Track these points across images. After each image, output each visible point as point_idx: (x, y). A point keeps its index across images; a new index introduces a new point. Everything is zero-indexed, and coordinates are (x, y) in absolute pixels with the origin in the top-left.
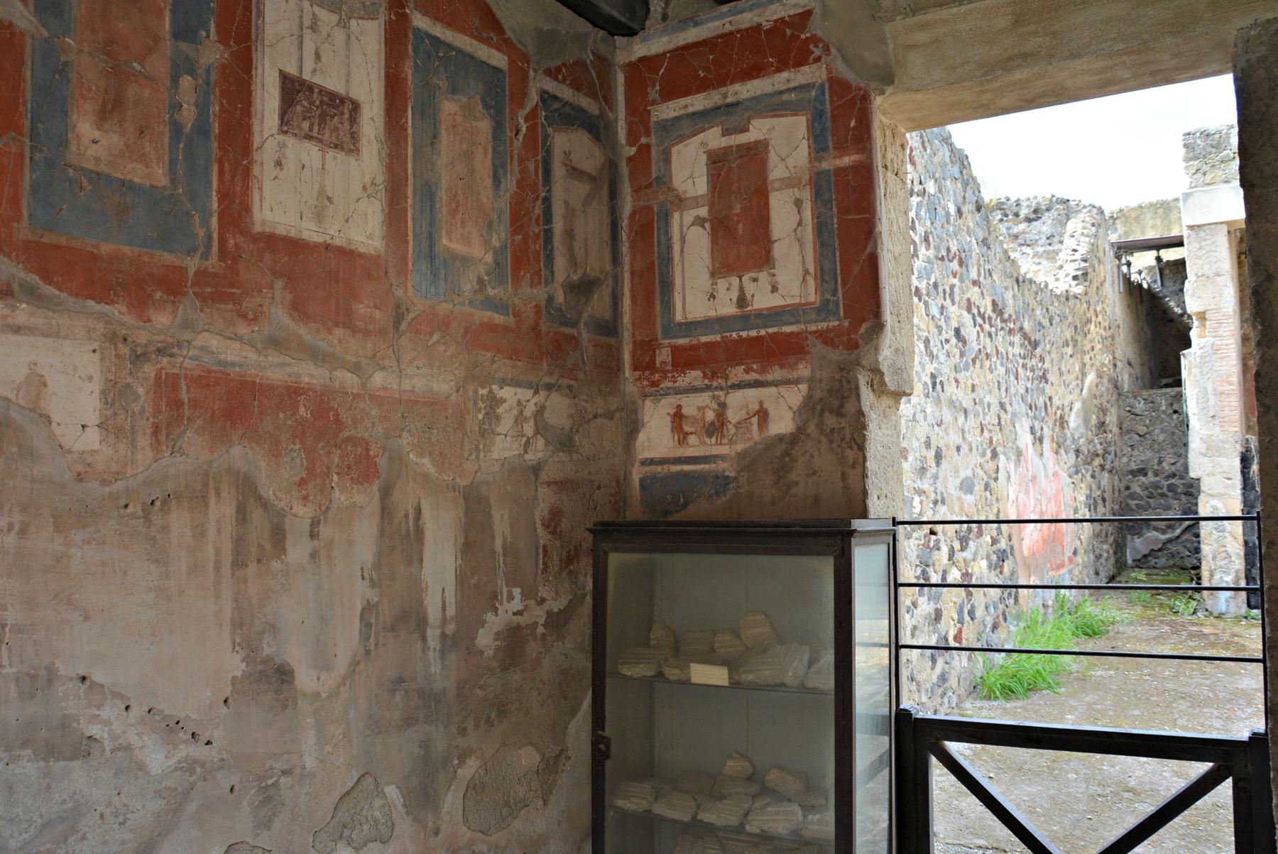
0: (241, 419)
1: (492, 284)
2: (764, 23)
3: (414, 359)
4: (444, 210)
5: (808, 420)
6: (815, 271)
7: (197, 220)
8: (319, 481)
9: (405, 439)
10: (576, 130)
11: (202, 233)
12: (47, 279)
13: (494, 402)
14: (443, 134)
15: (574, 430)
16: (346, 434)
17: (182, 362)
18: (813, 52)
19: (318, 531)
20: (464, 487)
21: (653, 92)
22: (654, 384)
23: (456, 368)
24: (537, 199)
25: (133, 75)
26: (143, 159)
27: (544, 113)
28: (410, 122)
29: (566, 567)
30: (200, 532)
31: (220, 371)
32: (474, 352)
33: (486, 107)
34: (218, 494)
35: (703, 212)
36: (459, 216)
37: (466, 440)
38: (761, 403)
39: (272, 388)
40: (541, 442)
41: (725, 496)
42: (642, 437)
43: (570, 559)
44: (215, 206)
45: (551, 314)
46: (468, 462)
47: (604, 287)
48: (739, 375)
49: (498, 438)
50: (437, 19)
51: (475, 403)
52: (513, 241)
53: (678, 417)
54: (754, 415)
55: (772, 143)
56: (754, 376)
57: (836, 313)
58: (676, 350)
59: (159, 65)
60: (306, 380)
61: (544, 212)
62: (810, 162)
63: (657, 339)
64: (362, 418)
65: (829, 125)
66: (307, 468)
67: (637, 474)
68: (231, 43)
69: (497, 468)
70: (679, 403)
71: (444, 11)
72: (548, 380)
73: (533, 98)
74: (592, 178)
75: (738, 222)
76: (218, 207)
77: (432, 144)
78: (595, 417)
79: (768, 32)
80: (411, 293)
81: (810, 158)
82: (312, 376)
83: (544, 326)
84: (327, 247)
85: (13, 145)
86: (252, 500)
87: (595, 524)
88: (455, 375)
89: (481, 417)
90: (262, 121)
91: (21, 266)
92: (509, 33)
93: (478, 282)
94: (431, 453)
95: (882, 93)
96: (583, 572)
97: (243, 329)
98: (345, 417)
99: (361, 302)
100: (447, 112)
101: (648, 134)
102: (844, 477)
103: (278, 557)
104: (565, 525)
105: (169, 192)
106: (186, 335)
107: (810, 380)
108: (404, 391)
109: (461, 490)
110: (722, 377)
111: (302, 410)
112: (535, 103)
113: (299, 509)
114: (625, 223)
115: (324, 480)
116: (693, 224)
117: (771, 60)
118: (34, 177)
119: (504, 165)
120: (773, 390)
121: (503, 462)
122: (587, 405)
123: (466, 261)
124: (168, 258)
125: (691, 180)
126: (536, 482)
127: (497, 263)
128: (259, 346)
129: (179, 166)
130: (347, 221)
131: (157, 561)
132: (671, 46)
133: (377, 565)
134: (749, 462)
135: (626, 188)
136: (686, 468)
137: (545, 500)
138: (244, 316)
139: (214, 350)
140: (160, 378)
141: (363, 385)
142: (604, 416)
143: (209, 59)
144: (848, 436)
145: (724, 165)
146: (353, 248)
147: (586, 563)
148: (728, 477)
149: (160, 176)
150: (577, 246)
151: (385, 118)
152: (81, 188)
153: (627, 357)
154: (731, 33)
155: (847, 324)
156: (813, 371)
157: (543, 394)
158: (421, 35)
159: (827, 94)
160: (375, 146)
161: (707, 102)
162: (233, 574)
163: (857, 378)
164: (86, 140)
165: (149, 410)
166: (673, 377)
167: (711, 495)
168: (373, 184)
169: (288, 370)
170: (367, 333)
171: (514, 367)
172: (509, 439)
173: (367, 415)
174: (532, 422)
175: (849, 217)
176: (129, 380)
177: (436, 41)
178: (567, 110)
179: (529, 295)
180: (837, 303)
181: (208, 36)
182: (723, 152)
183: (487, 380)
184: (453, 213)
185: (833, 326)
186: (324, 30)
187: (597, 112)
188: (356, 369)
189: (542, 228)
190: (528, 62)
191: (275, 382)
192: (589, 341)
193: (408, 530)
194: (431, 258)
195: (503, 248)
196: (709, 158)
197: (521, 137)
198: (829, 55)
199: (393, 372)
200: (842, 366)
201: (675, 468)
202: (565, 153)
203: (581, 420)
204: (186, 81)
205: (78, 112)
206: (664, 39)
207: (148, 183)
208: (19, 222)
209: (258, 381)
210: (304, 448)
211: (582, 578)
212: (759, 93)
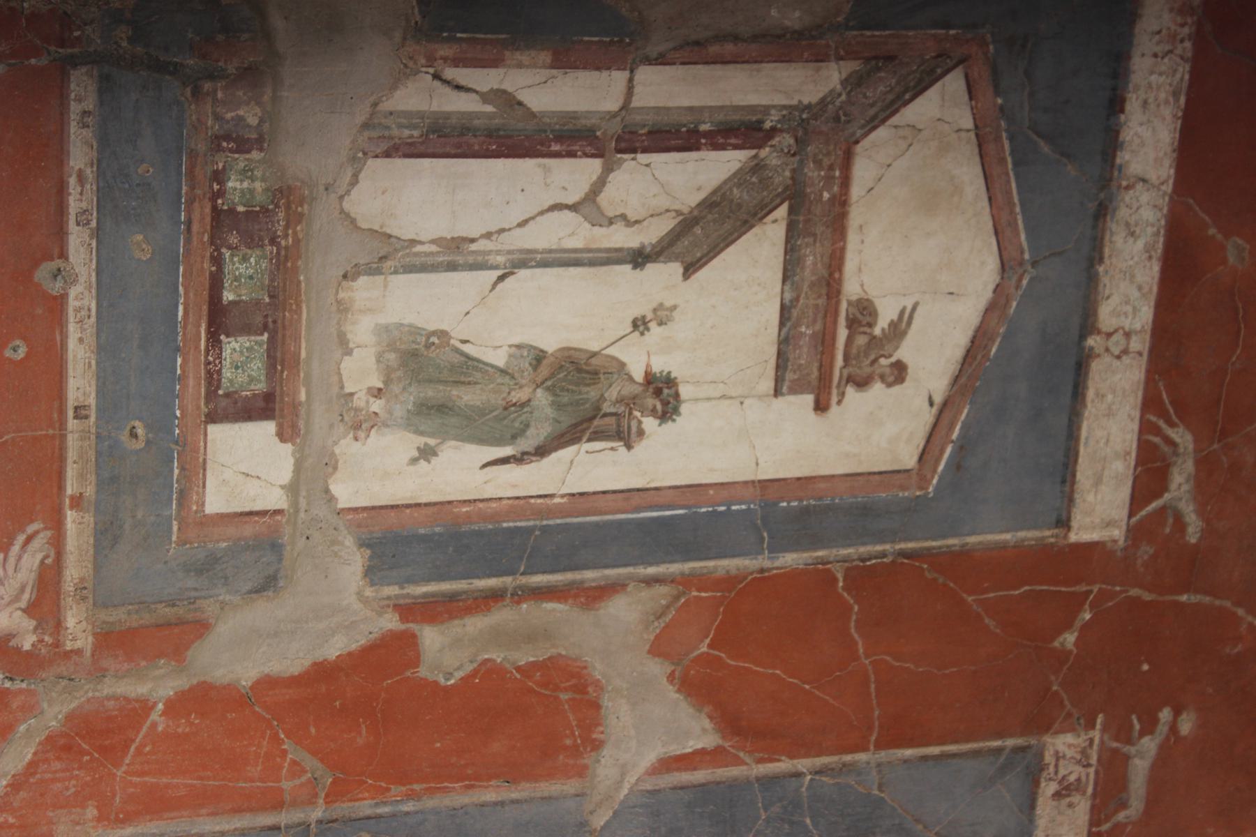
85: (297, 782)
208: (99, 819)
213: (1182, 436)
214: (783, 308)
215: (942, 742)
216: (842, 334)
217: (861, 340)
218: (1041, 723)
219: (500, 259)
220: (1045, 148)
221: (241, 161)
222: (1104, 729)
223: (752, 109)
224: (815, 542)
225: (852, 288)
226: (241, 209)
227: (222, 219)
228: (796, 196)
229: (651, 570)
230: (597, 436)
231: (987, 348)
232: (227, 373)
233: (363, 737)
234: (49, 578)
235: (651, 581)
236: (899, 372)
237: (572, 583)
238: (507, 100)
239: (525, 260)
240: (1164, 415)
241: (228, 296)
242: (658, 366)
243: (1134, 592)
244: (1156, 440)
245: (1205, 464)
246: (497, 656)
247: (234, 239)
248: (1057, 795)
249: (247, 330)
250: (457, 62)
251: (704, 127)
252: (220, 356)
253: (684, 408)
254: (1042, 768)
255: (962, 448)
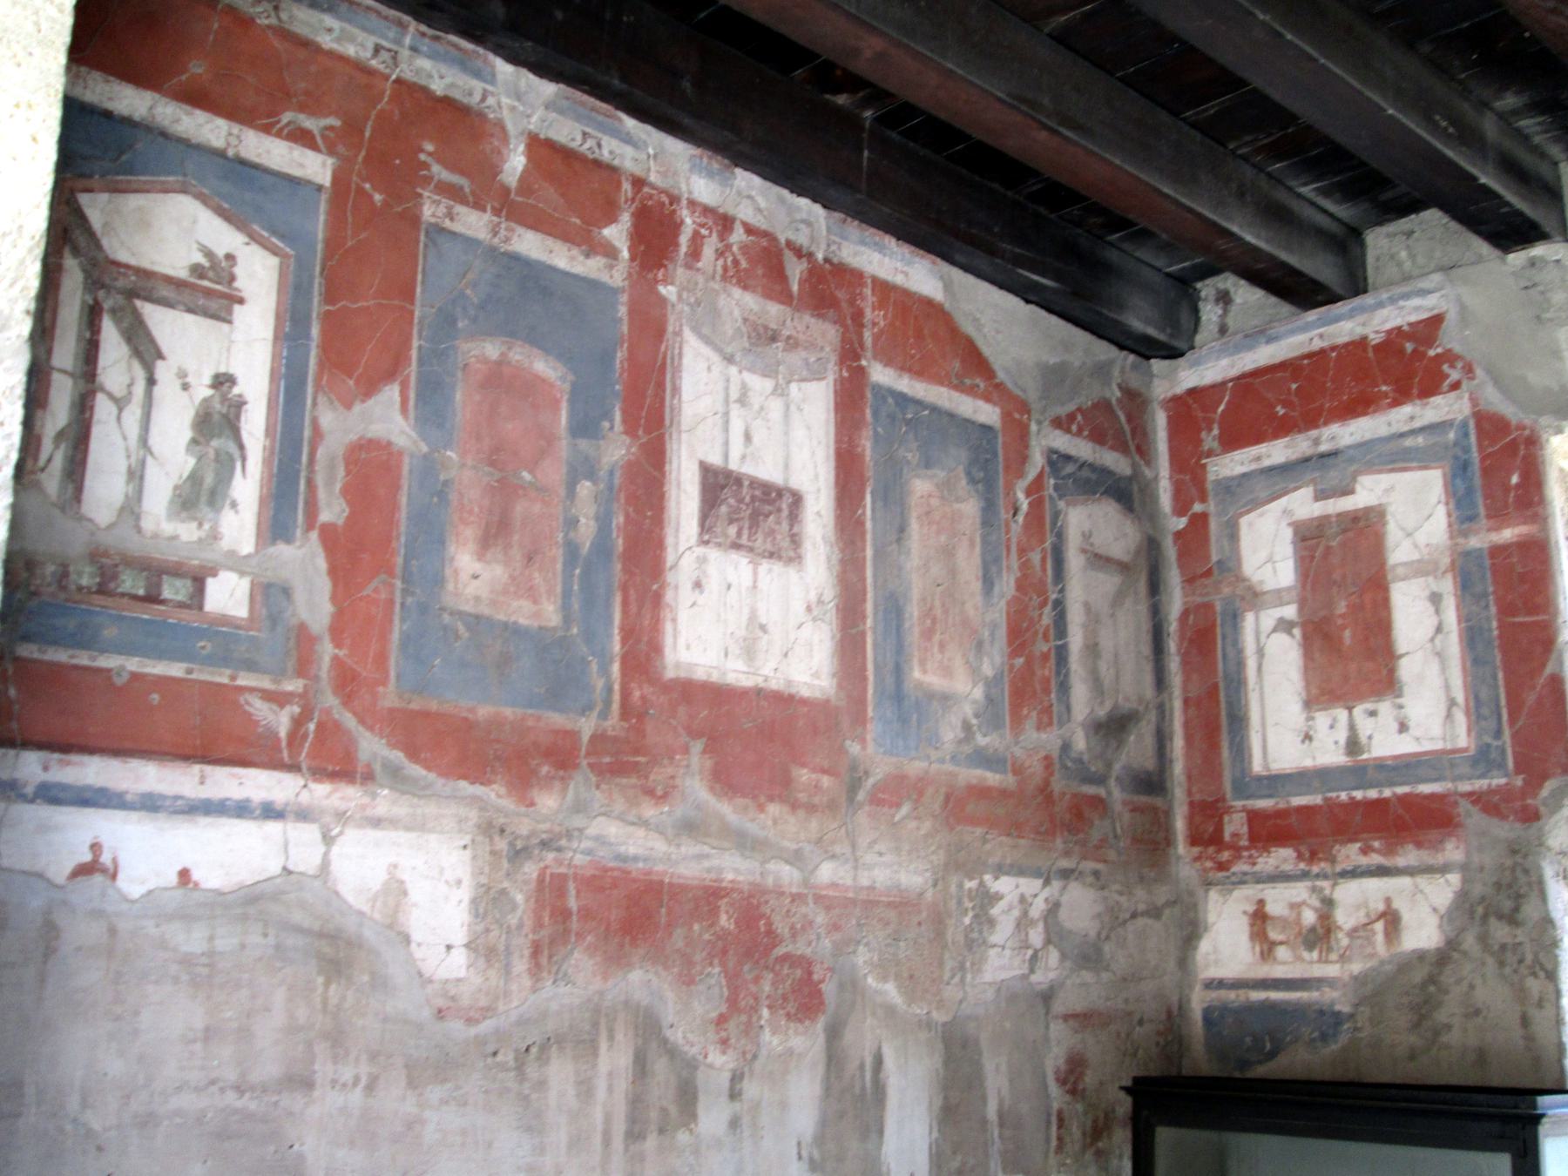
0: (643, 934)
1: (984, 730)
2: (1372, 336)
3: (875, 842)
4: (916, 630)
5: (1463, 930)
6: (1467, 700)
7: (594, 667)
8: (744, 1018)
9: (862, 957)
10: (1099, 499)
11: (600, 684)
12: (413, 754)
13: (987, 899)
14: (914, 526)
15: (1103, 936)
16: (780, 951)
17: (572, 858)
18: (1447, 376)
19: (741, 1089)
20: (944, 1024)
21: (1210, 439)
22: (1222, 867)
23: (933, 853)
24: (1043, 604)
25: (522, 487)
26: (532, 594)
27: (1052, 481)
28: (869, 512)
29: (1092, 1144)
30: (585, 1089)
31: (619, 869)
32: (959, 828)
33: (972, 481)
34: (611, 1038)
35: (1290, 612)
36: (937, 638)
37: (947, 956)
38: (1388, 901)
39: (684, 888)
40: (1053, 956)
41: (1336, 1042)
42: (1205, 946)
43: (1097, 1132)
44: (617, 647)
45: (1067, 768)
46: (950, 987)
47: (1144, 723)
48: (1353, 857)
49: (992, 952)
50: (904, 368)
51: (960, 903)
52: (1012, 667)
53: (1259, 917)
54: (1378, 919)
55: (1391, 509)
56: (1376, 859)
57: (1501, 765)
58: (1254, 817)
59: (553, 473)
60: (730, 876)
61: (1056, 622)
62: (1452, 537)
63: (1223, 799)
64: (803, 928)
65: (1478, 481)
66: (728, 1000)
67: (1198, 1001)
68: (640, 432)
69: (990, 995)
70: (1260, 896)
71: (912, 357)
72: (1065, 863)
73: (1037, 461)
74: (1124, 567)
75: (1343, 628)
76: (622, 648)
77: (899, 540)
78: (1134, 916)
79: (1378, 348)
80: (871, 748)
81: (1451, 532)
82: (736, 871)
83: (1058, 785)
84: (759, 692)
86: (654, 1045)
87: (1136, 1080)
88: (932, 862)
89: (967, 920)
90: (677, 530)
91: (384, 741)
92: (1001, 376)
93: (963, 727)
94: (897, 977)
95: (1559, 431)
96: (1117, 1152)
97: (649, 811)
98: (781, 927)
99: (803, 765)
100: (919, 494)
101: (1203, 499)
102: (1525, 1021)
103: (686, 1125)
104: (1090, 1080)
105: (560, 633)
106: (578, 821)
107: (1464, 868)
108: (862, 888)
109: (940, 1029)
110: (1326, 860)
111: (724, 920)
112: (1038, 470)
113: (716, 1058)
114: (1173, 626)
115: (750, 1017)
116: (1275, 630)
117: (1384, 388)
118: (405, 627)
119: (997, 560)
120: (1405, 882)
121: (999, 987)
122: (1123, 899)
123: (946, 699)
124: (557, 719)
125: (1269, 565)
126: (1047, 1013)
127: (989, 699)
128: (670, 831)
129: (573, 599)
130: (786, 655)
131: (529, 1129)
132: (1234, 372)
133: (819, 1140)
134: (1372, 991)
135: (1173, 577)
136: (1275, 995)
137: (1059, 1043)
138: (650, 792)
139: (613, 840)
140: (543, 881)
141: (805, 883)
142: (1146, 913)
143: (612, 456)
144: (1529, 958)
145: (1318, 545)
146: (793, 691)
147: (1121, 1139)
148: (1339, 1013)
149: (551, 614)
150: (1103, 667)
151: (836, 510)
152: (458, 637)
153: (1180, 825)
154: (1322, 352)
155: (1519, 781)
156: (1468, 853)
157: (1056, 884)
158: (883, 393)
159: (1473, 438)
160: (823, 550)
161: (1290, 451)
162: (626, 1149)
163: (1539, 868)
164: (464, 576)
165: (529, 923)
166: (1250, 857)
167: (1313, 1040)
168: (820, 602)
169: (706, 864)
170: (811, 809)
171: (1015, 847)
172: (1007, 952)
173: (811, 923)
174: (1040, 927)
175: (1517, 620)
176: (506, 884)
177: (902, 399)
178: (1085, 473)
179: (1036, 741)
180: (1503, 751)
181: (612, 428)
182: (1315, 523)
183: (974, 868)
184: (928, 634)
185: (1498, 786)
186: (755, 400)
187: (1128, 471)
188: (796, 858)
189: (1053, 644)
190: (1029, 412)
191: (690, 882)
192: (1124, 803)
193: (863, 1088)
194: (898, 697)
195: (997, 679)
196: (1296, 533)
197: (1020, 518)
198: (1473, 379)
199: (847, 861)
200: (1517, 847)
201: (1257, 996)
202: (1083, 534)
203: (1114, 920)
204: (585, 488)
205: (457, 541)
206: (1224, 362)
207: (536, 624)
209: (667, 880)
210: (726, 972)
211: (1115, 1162)
212: (1368, 436)
213: (287, 117)
214: (190, 310)
215: (415, 273)
216: (205, 283)
217: (211, 274)
218: (414, 220)
219: (142, 453)
220: (124, 158)
221: (73, 577)
222: (423, 189)
223: (82, 309)
224: (308, 317)
225: (183, 274)
226: (98, 580)
227: (102, 590)
228: (132, 294)
229: (309, 402)
230: (238, 417)
231: (225, 210)
232: (180, 598)
233: (366, 556)
234: (268, 696)
235: (315, 404)
236: (230, 257)
237: (310, 442)
238: (60, 436)
239: (144, 441)
240: (272, 125)
241: (141, 592)
242: (207, 380)
243: (360, 159)
244: (286, 131)
245: (302, 108)
246: (338, 486)
247: (112, 585)
248: (452, 219)
249: (159, 585)
250: (36, 459)
251: (88, 335)
252: (171, 601)
253: (231, 371)
254: (436, 225)
255: (274, 233)
